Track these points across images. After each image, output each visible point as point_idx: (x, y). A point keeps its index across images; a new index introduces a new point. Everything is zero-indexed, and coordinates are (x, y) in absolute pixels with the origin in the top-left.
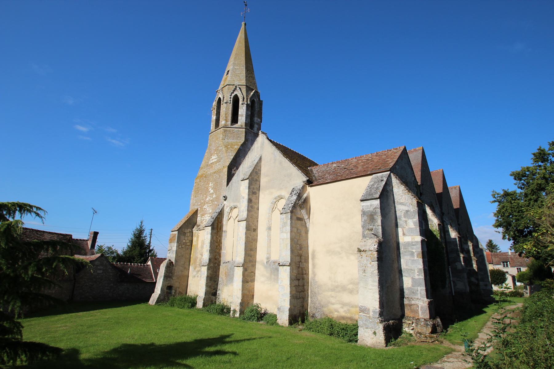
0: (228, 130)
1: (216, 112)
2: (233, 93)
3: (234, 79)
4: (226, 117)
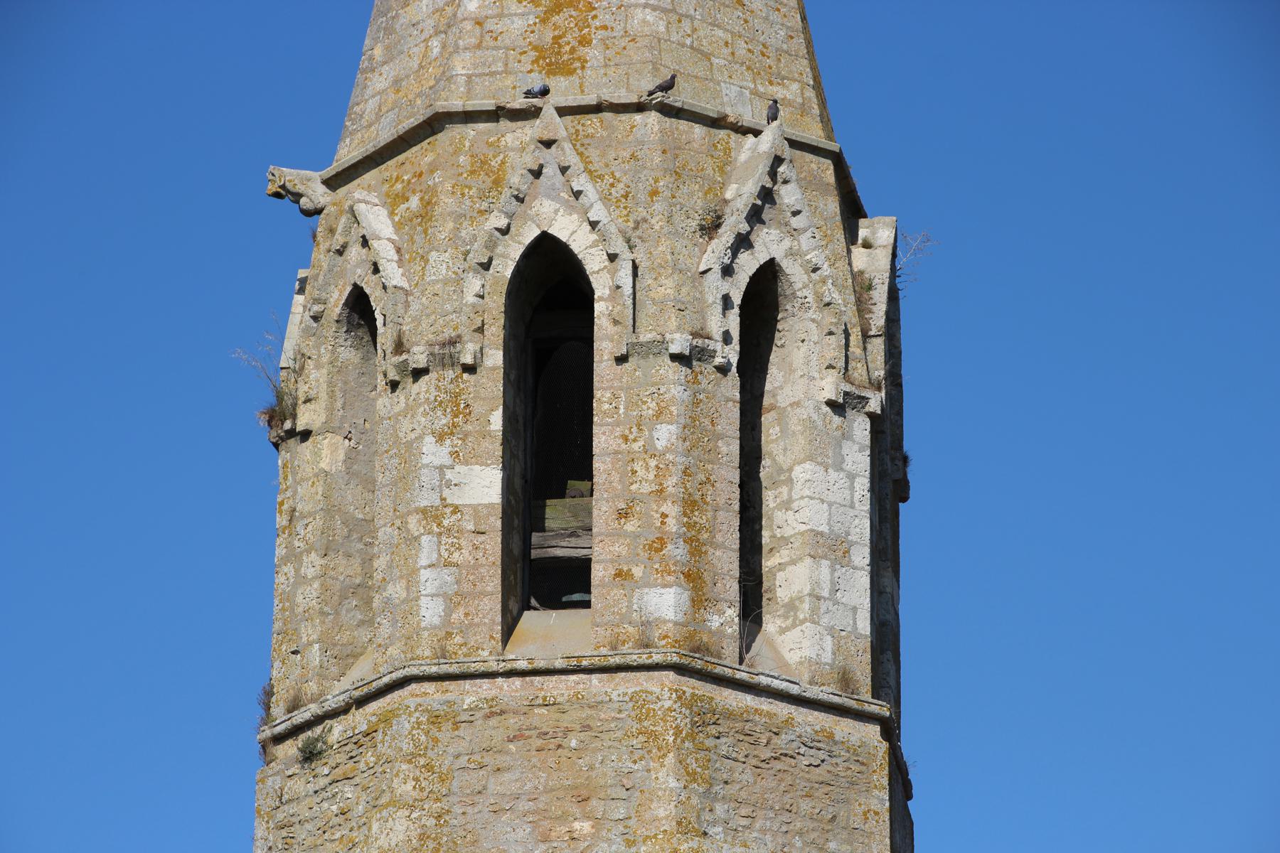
0: (729, 715)
1: (497, 421)
2: (743, 242)
3: (711, 37)
4: (696, 547)
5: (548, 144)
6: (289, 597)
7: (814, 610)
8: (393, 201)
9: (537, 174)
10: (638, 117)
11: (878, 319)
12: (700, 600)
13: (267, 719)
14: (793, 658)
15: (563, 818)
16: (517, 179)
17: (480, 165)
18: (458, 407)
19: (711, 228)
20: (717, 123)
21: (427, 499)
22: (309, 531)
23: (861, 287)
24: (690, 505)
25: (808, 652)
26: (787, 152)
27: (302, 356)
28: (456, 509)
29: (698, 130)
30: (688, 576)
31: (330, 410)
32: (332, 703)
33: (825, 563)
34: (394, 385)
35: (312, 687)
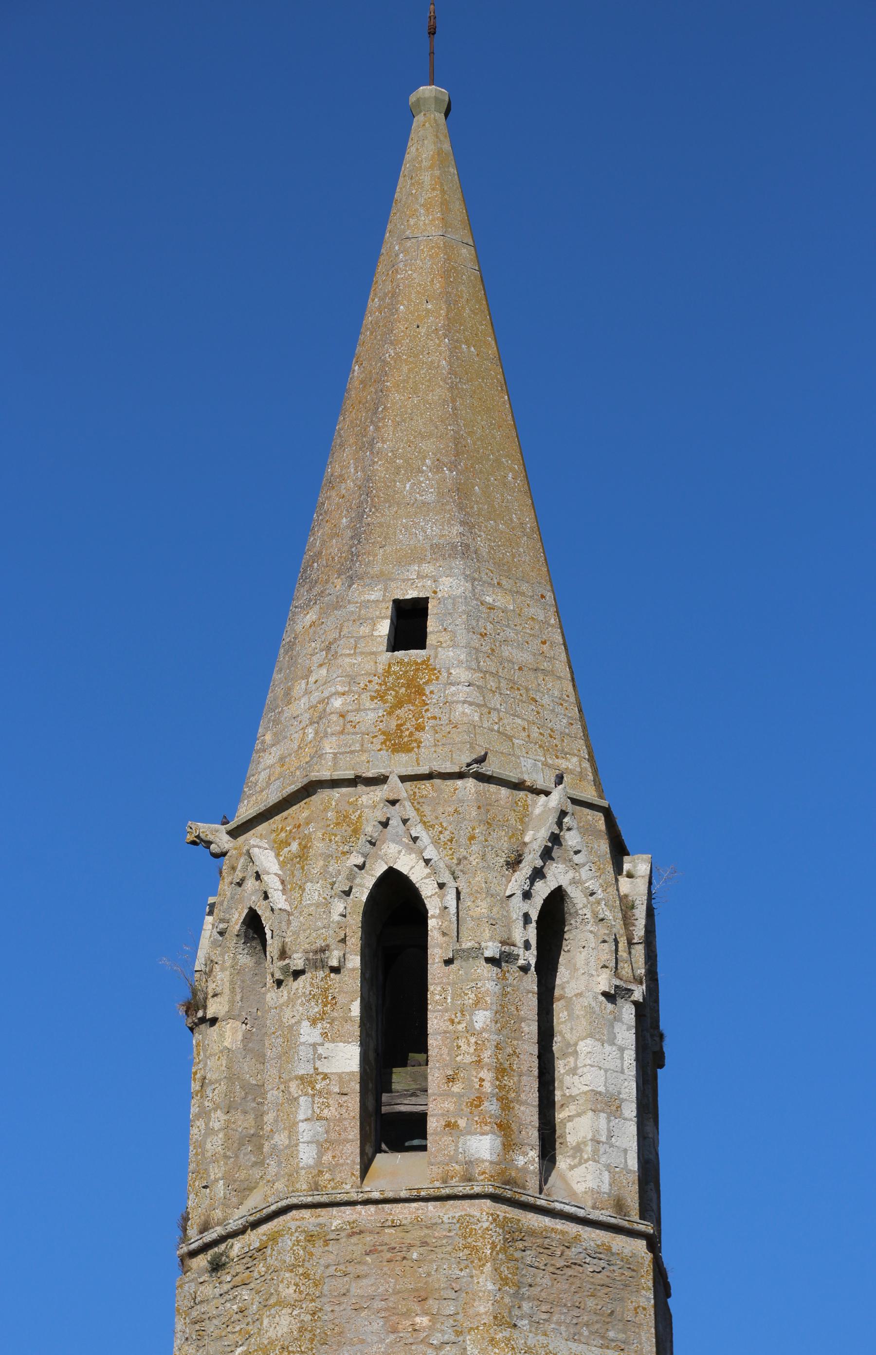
0: (532, 1233)
1: (356, 1009)
2: (538, 874)
3: (513, 724)
4: (506, 1104)
5: (393, 802)
6: (201, 1145)
7: (595, 1152)
8: (279, 846)
9: (385, 824)
10: (459, 783)
11: (639, 931)
12: (509, 1144)
13: (185, 1238)
14: (579, 1188)
15: (407, 1314)
16: (370, 828)
17: (344, 818)
18: (326, 998)
19: (514, 863)
20: (518, 786)
21: (303, 1069)
22: (216, 1094)
23: (626, 907)
24: (501, 1071)
25: (591, 1184)
26: (570, 807)
27: (211, 962)
28: (326, 1076)
29: (504, 792)
30: (500, 1126)
31: (232, 1002)
32: (233, 1226)
33: (603, 1115)
34: (279, 983)
35: (218, 1214)
